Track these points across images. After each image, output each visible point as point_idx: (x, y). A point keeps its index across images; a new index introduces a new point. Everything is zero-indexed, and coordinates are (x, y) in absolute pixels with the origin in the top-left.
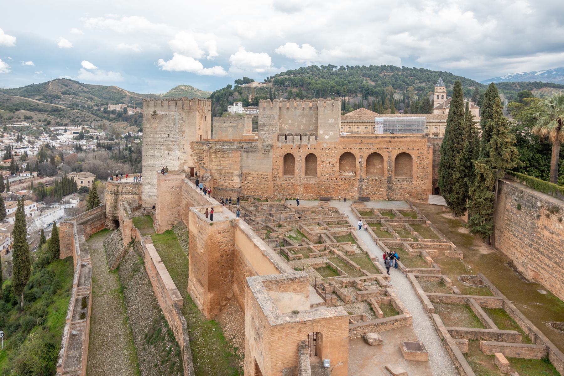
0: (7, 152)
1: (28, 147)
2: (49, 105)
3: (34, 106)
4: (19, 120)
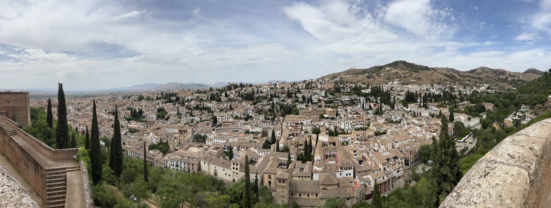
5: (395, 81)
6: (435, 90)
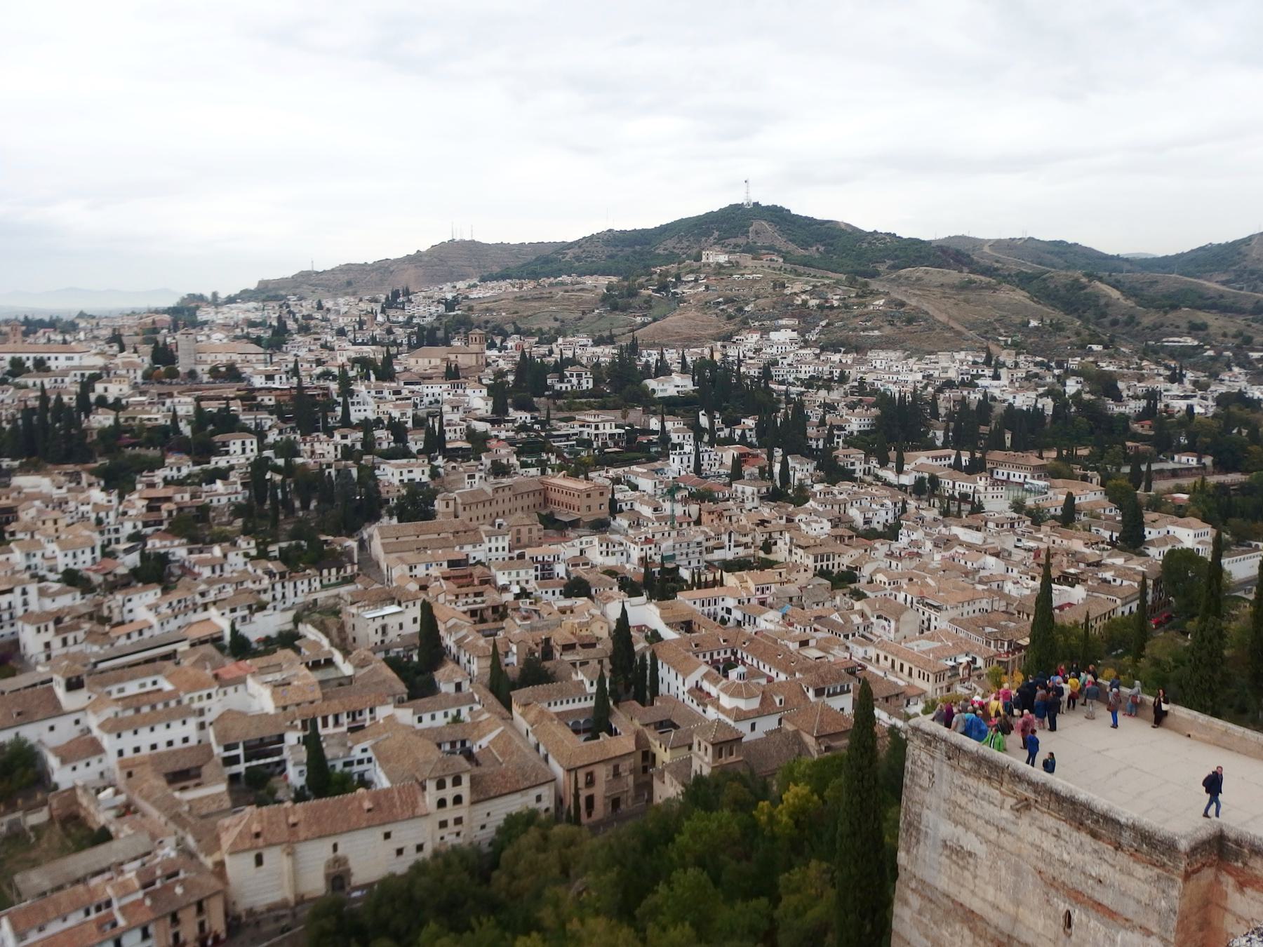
0: (1149, 404)
1: (1195, 396)
2: (1250, 296)
3: (1211, 298)
4: (1177, 330)
5: (777, 329)
6: (1004, 381)
